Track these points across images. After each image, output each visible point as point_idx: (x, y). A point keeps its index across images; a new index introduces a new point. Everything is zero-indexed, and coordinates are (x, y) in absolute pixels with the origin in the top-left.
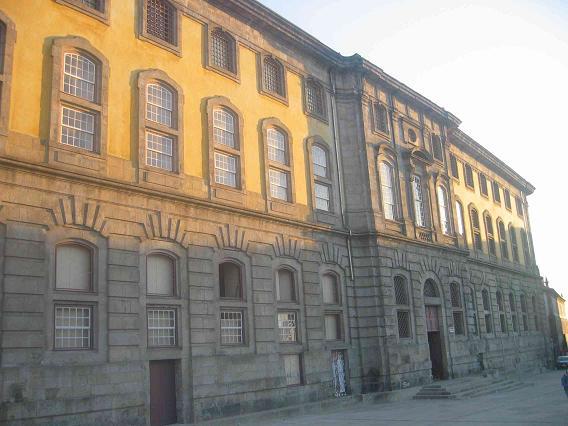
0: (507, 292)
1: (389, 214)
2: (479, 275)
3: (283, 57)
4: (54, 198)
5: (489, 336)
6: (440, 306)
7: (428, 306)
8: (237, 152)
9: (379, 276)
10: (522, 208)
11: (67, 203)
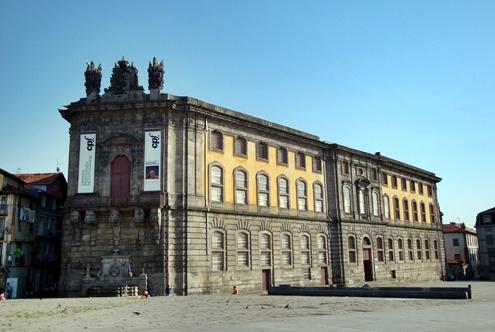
1: (347, 210)
3: (304, 150)
5: (401, 262)
7: (364, 249)
10: (432, 191)
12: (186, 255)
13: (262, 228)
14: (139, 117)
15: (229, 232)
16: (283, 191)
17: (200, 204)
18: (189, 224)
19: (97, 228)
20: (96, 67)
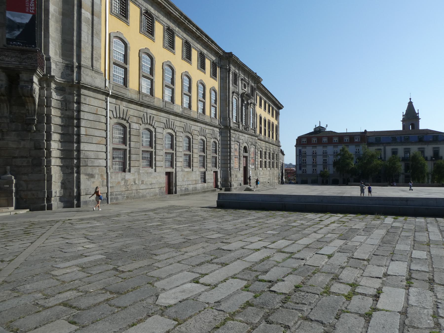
0: (268, 151)
2: (260, 144)
4: (142, 113)
6: (247, 157)
7: (244, 157)
8: (190, 94)
9: (230, 144)
11: (145, 115)
12: (79, 150)
13: (167, 126)
15: (134, 126)
16: (186, 90)
17: (98, 82)
18: (83, 108)
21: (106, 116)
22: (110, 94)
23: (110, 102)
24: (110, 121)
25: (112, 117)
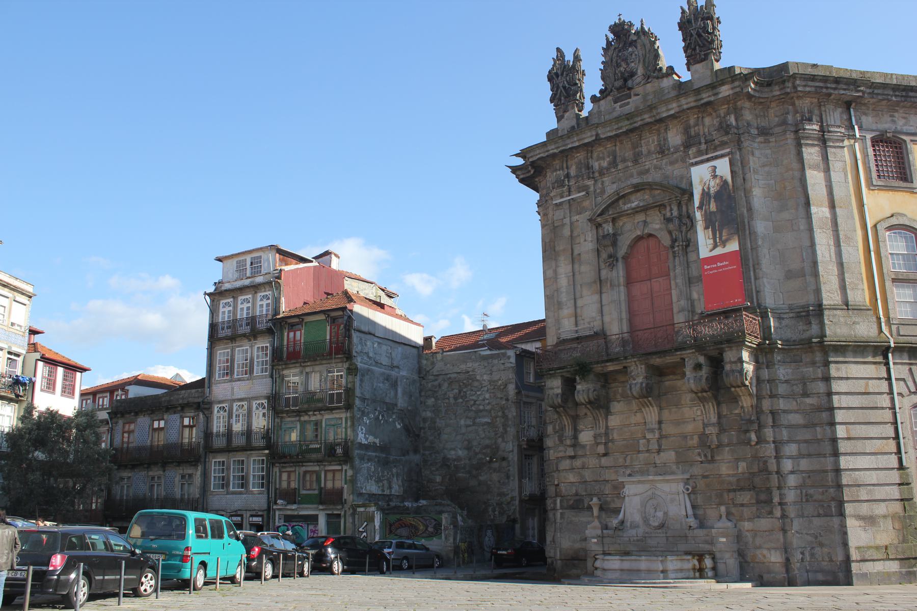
12: (838, 471)
14: (675, 138)
17: (865, 330)
18: (836, 386)
19: (608, 412)
20: (569, 57)
21: (891, 392)
22: (892, 345)
23: (894, 363)
24: (900, 402)
25: (905, 391)
